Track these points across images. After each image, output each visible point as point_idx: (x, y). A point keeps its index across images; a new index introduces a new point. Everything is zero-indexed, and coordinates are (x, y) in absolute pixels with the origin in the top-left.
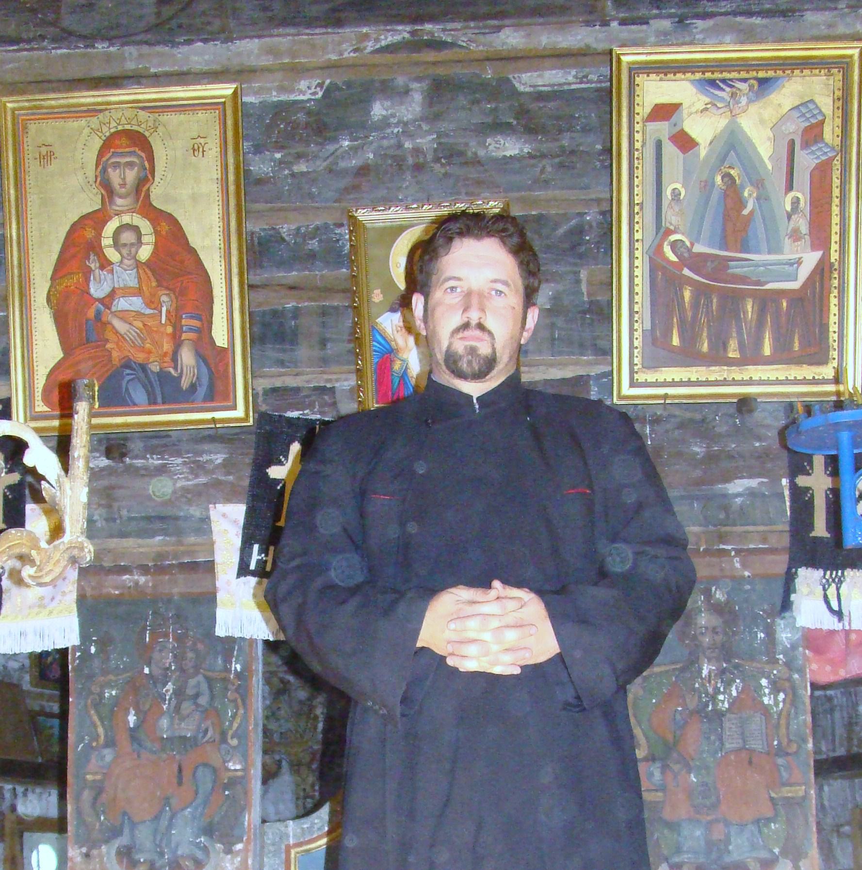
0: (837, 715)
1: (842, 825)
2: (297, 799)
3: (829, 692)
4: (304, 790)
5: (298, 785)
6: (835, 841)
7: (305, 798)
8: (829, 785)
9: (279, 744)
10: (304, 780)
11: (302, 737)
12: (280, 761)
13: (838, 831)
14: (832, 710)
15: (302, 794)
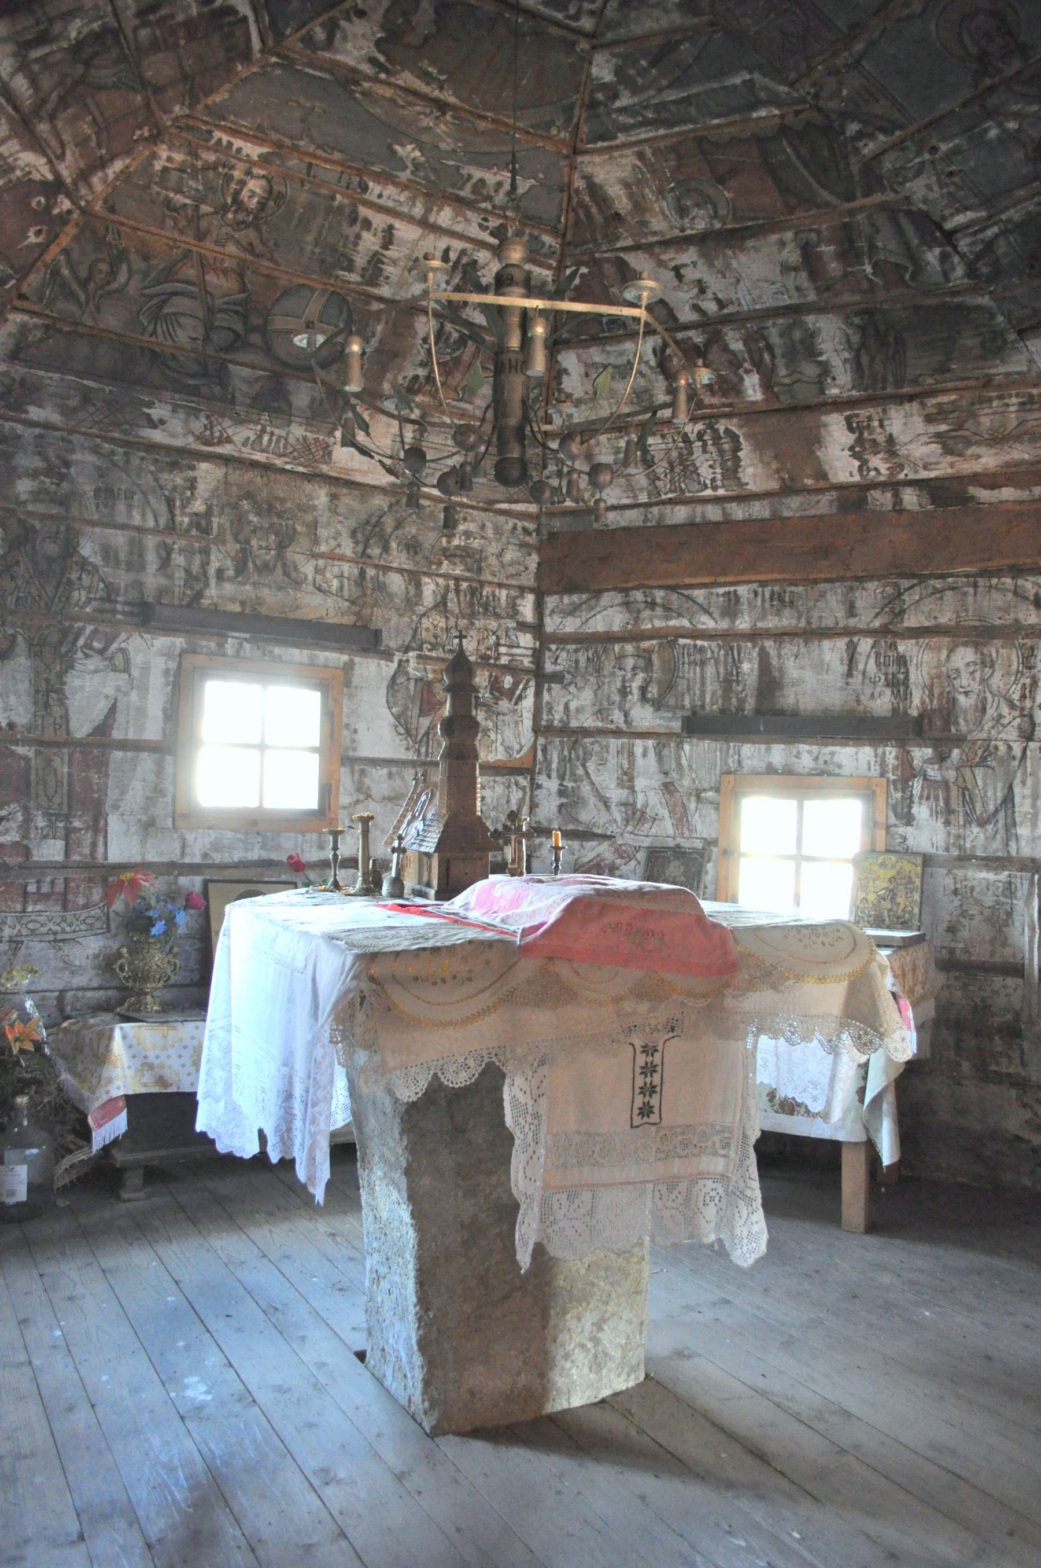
0: (710, 670)
1: (704, 790)
2: (37, 692)
3: (699, 643)
4: (47, 681)
5: (37, 673)
6: (692, 805)
7: (47, 692)
8: (692, 745)
9: (12, 613)
10: (48, 667)
11: (48, 607)
12: (14, 637)
13: (698, 798)
14: (703, 663)
15: (44, 685)
